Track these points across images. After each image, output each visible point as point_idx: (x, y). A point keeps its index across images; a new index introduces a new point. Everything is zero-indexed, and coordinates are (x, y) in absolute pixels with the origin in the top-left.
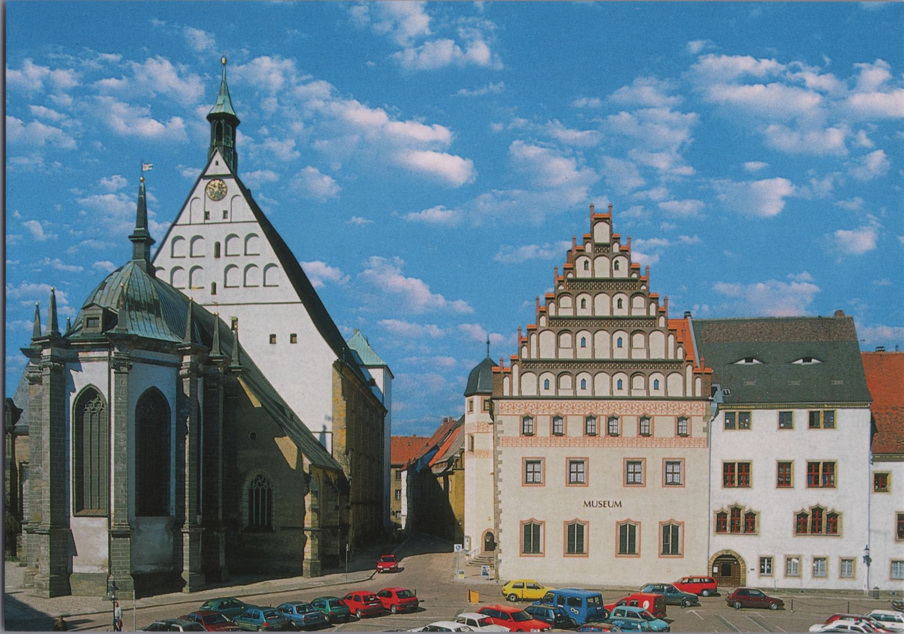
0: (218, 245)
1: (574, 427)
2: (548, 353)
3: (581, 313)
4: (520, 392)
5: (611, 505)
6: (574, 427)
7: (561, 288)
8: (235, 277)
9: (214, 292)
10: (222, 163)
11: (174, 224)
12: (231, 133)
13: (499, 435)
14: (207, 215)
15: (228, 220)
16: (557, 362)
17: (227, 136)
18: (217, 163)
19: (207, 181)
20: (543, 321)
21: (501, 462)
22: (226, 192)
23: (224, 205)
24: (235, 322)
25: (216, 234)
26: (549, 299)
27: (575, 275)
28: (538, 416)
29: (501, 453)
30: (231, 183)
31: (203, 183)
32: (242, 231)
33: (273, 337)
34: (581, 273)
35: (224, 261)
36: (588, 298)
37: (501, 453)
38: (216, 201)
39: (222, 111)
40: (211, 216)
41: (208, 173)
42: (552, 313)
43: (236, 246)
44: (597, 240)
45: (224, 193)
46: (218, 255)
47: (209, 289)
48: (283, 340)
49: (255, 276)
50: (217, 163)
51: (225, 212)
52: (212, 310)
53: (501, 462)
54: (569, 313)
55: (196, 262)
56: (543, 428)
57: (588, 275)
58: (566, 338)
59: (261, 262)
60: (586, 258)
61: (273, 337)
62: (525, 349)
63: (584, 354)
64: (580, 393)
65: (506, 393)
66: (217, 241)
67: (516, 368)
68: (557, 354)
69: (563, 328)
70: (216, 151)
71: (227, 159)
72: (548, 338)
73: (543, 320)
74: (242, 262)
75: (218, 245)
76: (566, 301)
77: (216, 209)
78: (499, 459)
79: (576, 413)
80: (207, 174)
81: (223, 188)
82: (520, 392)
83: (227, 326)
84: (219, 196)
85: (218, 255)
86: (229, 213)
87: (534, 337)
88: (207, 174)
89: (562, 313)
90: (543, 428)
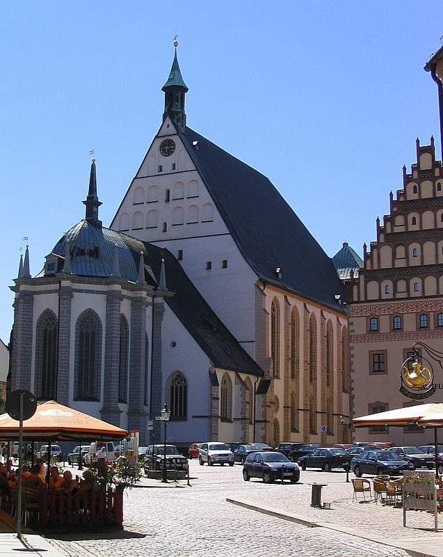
1: (410, 324)
2: (386, 264)
3: (412, 228)
4: (366, 296)
5: (441, 387)
6: (410, 324)
7: (395, 209)
9: (165, 231)
10: (172, 126)
13: (351, 334)
16: (394, 269)
18: (168, 125)
19: (162, 139)
20: (382, 240)
21: (353, 356)
24: (181, 252)
26: (386, 219)
27: (405, 198)
28: (381, 317)
29: (353, 348)
30: (176, 139)
34: (412, 196)
36: (416, 215)
37: (353, 348)
42: (389, 231)
44: (423, 168)
46: (168, 200)
47: (161, 227)
48: (216, 266)
50: (168, 125)
51: (174, 165)
52: (162, 245)
53: (353, 356)
54: (402, 229)
56: (385, 327)
57: (416, 197)
58: (400, 251)
60: (415, 184)
62: (368, 262)
63: (415, 262)
64: (413, 294)
65: (355, 299)
66: (167, 188)
67: (362, 277)
68: (393, 264)
69: (397, 243)
72: (386, 251)
73: (382, 236)
76: (399, 220)
77: (167, 162)
78: (352, 353)
79: (410, 312)
82: (366, 296)
83: (175, 258)
85: (168, 200)
87: (375, 251)
89: (397, 230)
90: (385, 327)
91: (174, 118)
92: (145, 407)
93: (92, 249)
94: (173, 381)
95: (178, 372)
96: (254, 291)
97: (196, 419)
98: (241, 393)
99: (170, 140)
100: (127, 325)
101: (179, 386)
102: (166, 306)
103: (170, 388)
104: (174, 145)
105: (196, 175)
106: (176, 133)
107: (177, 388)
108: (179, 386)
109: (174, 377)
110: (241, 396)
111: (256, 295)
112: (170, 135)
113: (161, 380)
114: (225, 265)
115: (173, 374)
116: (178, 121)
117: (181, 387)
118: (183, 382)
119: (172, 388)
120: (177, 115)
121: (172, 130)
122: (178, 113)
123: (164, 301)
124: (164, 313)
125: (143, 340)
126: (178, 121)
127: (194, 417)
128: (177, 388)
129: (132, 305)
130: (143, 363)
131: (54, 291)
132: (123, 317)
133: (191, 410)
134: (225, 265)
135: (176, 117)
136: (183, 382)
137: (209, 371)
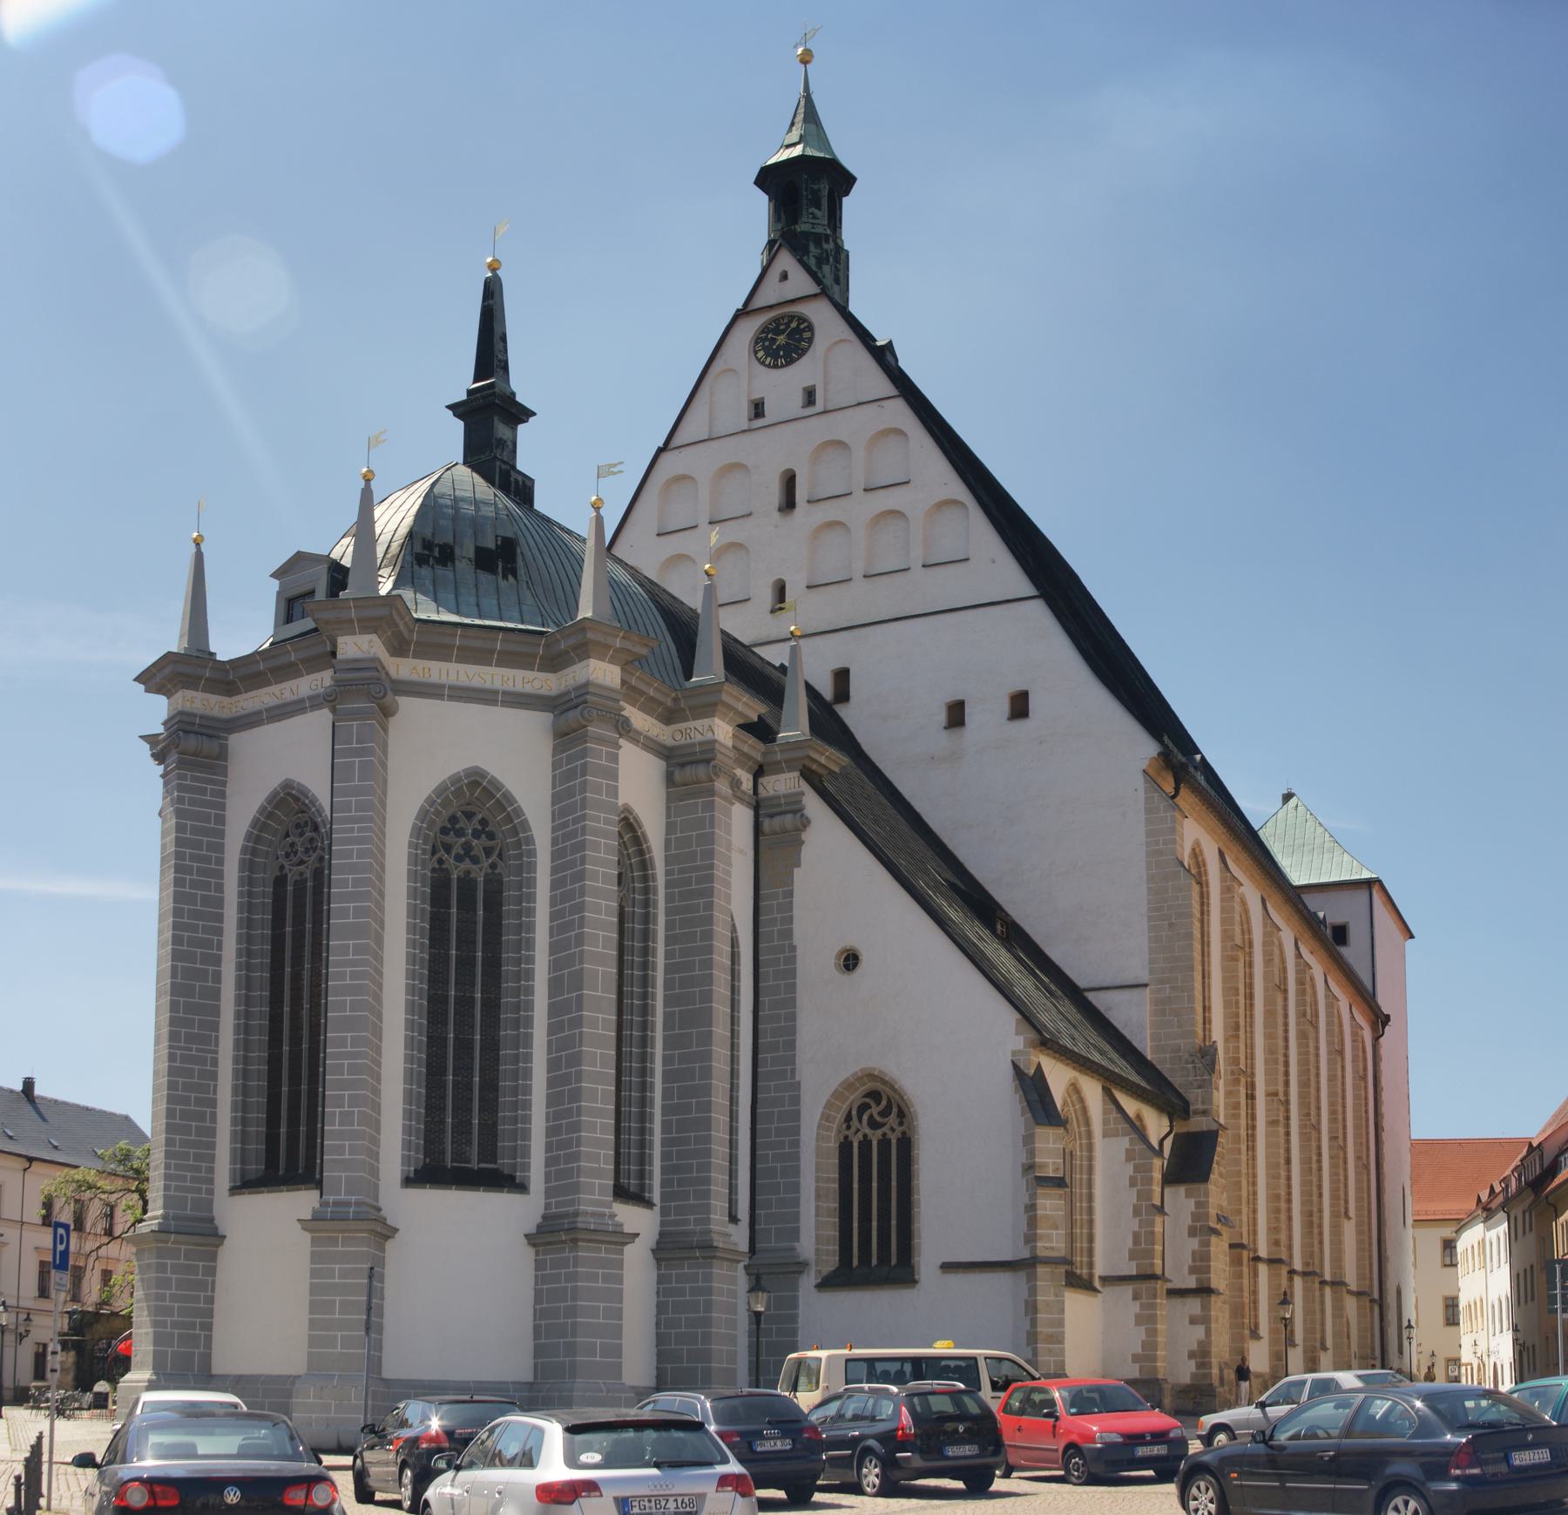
12: (825, 202)
17: (813, 210)
18: (784, 276)
38: (783, 366)
71: (812, 262)
81: (804, 330)
91: (807, 252)
92: (731, 1228)
94: (848, 1118)
95: (871, 1076)
96: (1141, 795)
99: (792, 317)
100: (645, 864)
101: (875, 1137)
102: (814, 805)
103: (833, 1145)
104: (810, 328)
106: (815, 289)
107: (865, 1144)
108: (875, 1137)
109: (855, 1098)
111: (1148, 811)
112: (793, 301)
113: (796, 1116)
115: (849, 1085)
116: (821, 261)
117: (884, 1143)
118: (893, 1119)
119: (845, 1148)
120: (818, 244)
121: (800, 283)
122: (819, 239)
123: (805, 787)
124: (804, 836)
125: (721, 930)
126: (821, 261)
128: (865, 1144)
129: (670, 780)
130: (721, 1030)
132: (629, 826)
133: (931, 1247)
135: (812, 247)
136: (893, 1119)
137: (1015, 1066)
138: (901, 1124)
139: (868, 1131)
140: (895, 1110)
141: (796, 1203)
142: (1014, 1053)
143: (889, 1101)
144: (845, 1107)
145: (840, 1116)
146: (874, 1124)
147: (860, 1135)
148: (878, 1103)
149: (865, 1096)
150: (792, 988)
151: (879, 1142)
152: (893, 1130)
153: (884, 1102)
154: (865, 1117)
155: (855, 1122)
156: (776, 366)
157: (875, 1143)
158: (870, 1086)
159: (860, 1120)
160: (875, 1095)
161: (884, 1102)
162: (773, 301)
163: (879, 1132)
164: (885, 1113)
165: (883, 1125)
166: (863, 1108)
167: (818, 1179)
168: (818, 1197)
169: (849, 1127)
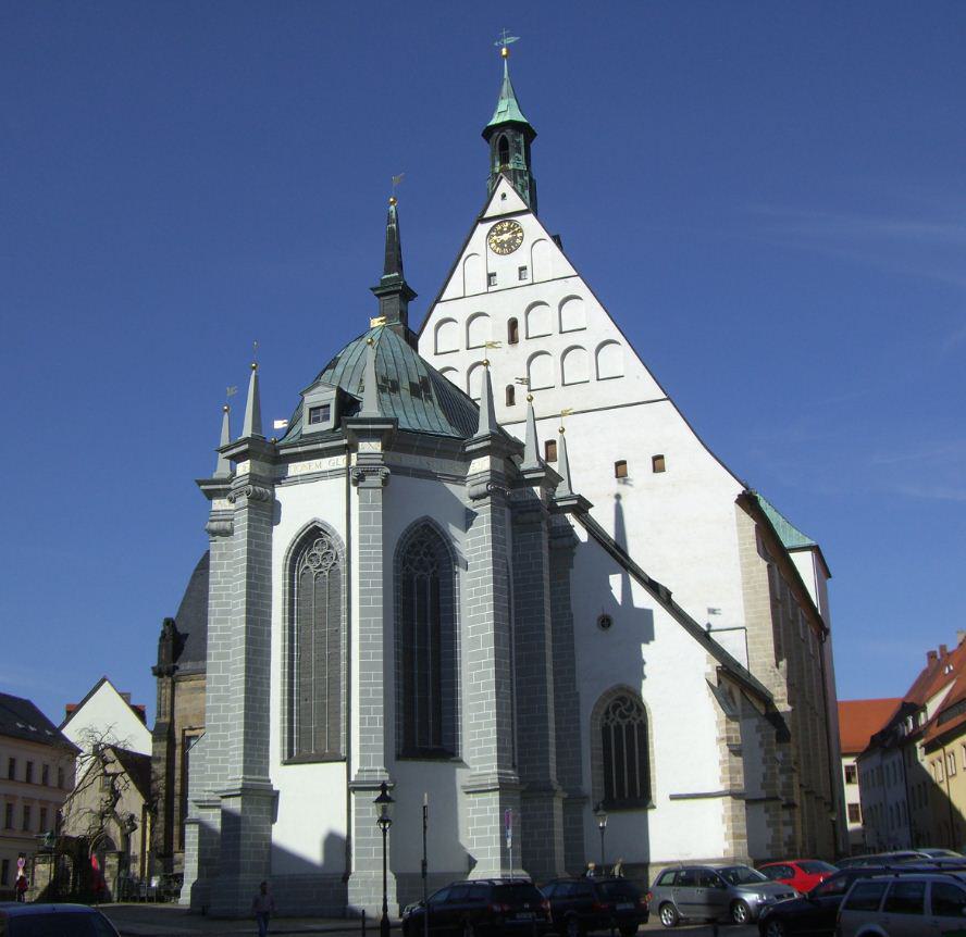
0: (513, 324)
8: (544, 372)
11: (438, 301)
14: (491, 276)
15: (529, 281)
17: (517, 155)
18: (504, 196)
22: (522, 238)
23: (520, 257)
25: (509, 305)
31: (483, 230)
32: (553, 293)
33: (620, 467)
35: (525, 348)
39: (507, 118)
40: (498, 279)
41: (488, 214)
43: (542, 321)
45: (518, 241)
46: (513, 340)
48: (639, 470)
49: (579, 366)
50: (504, 196)
51: (522, 269)
55: (479, 356)
59: (589, 341)
61: (620, 467)
70: (501, 178)
71: (519, 188)
74: (557, 344)
75: (513, 324)
77: (506, 267)
80: (488, 214)
84: (509, 247)
85: (513, 340)
86: (529, 269)
88: (485, 216)
93: (416, 380)
94: (607, 713)
95: (621, 688)
97: (675, 802)
98: (759, 737)
105: (578, 286)
107: (618, 728)
110: (761, 745)
114: (658, 463)
115: (608, 694)
119: (606, 730)
120: (522, 177)
122: (521, 173)
127: (674, 797)
128: (618, 728)
131: (334, 473)
134: (658, 463)
138: (639, 715)
139: (619, 720)
140: (635, 708)
141: (579, 762)
142: (706, 674)
143: (632, 705)
144: (605, 706)
145: (602, 712)
146: (623, 716)
147: (615, 723)
148: (625, 704)
149: (617, 700)
150: (571, 638)
151: (626, 726)
152: (634, 719)
153: (628, 704)
154: (617, 712)
155: (611, 716)
156: (502, 254)
157: (624, 727)
158: (620, 694)
159: (614, 713)
160: (622, 699)
161: (628, 704)
162: (498, 213)
163: (627, 720)
164: (630, 709)
165: (629, 716)
166: (615, 707)
167: (592, 749)
168: (592, 758)
169: (608, 718)
